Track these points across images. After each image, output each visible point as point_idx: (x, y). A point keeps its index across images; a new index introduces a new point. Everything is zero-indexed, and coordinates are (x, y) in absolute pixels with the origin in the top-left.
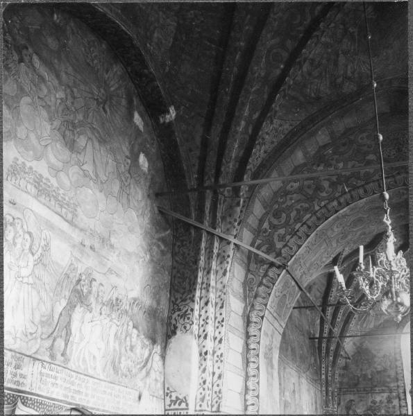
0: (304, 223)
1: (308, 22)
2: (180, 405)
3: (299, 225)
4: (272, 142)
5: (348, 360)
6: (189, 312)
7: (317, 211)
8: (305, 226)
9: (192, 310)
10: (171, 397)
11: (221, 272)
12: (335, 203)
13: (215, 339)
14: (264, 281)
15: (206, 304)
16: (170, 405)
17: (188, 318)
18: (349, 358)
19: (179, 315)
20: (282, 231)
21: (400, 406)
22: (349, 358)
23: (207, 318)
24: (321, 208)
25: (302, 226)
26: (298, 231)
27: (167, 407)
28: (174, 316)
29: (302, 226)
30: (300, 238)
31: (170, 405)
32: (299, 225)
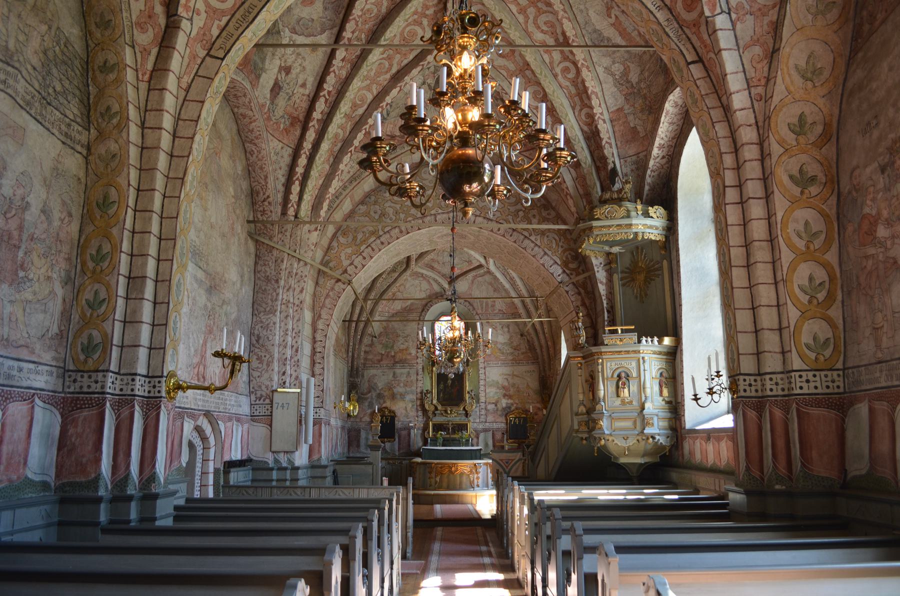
0: (369, 246)
1: (394, 70)
2: (264, 401)
3: (364, 246)
4: (349, 172)
5: (374, 339)
6: (271, 324)
7: (381, 236)
8: (370, 248)
9: (274, 323)
10: (256, 394)
11: (298, 290)
12: (397, 230)
13: (292, 347)
14: (331, 293)
15: (287, 317)
16: (255, 401)
17: (271, 330)
18: (375, 337)
19: (262, 327)
20: (349, 251)
21: (417, 380)
22: (375, 337)
23: (287, 330)
24: (385, 233)
25: (367, 247)
26: (363, 252)
27: (253, 403)
28: (257, 327)
29: (367, 247)
30: (364, 258)
31: (255, 401)
32: (364, 246)
